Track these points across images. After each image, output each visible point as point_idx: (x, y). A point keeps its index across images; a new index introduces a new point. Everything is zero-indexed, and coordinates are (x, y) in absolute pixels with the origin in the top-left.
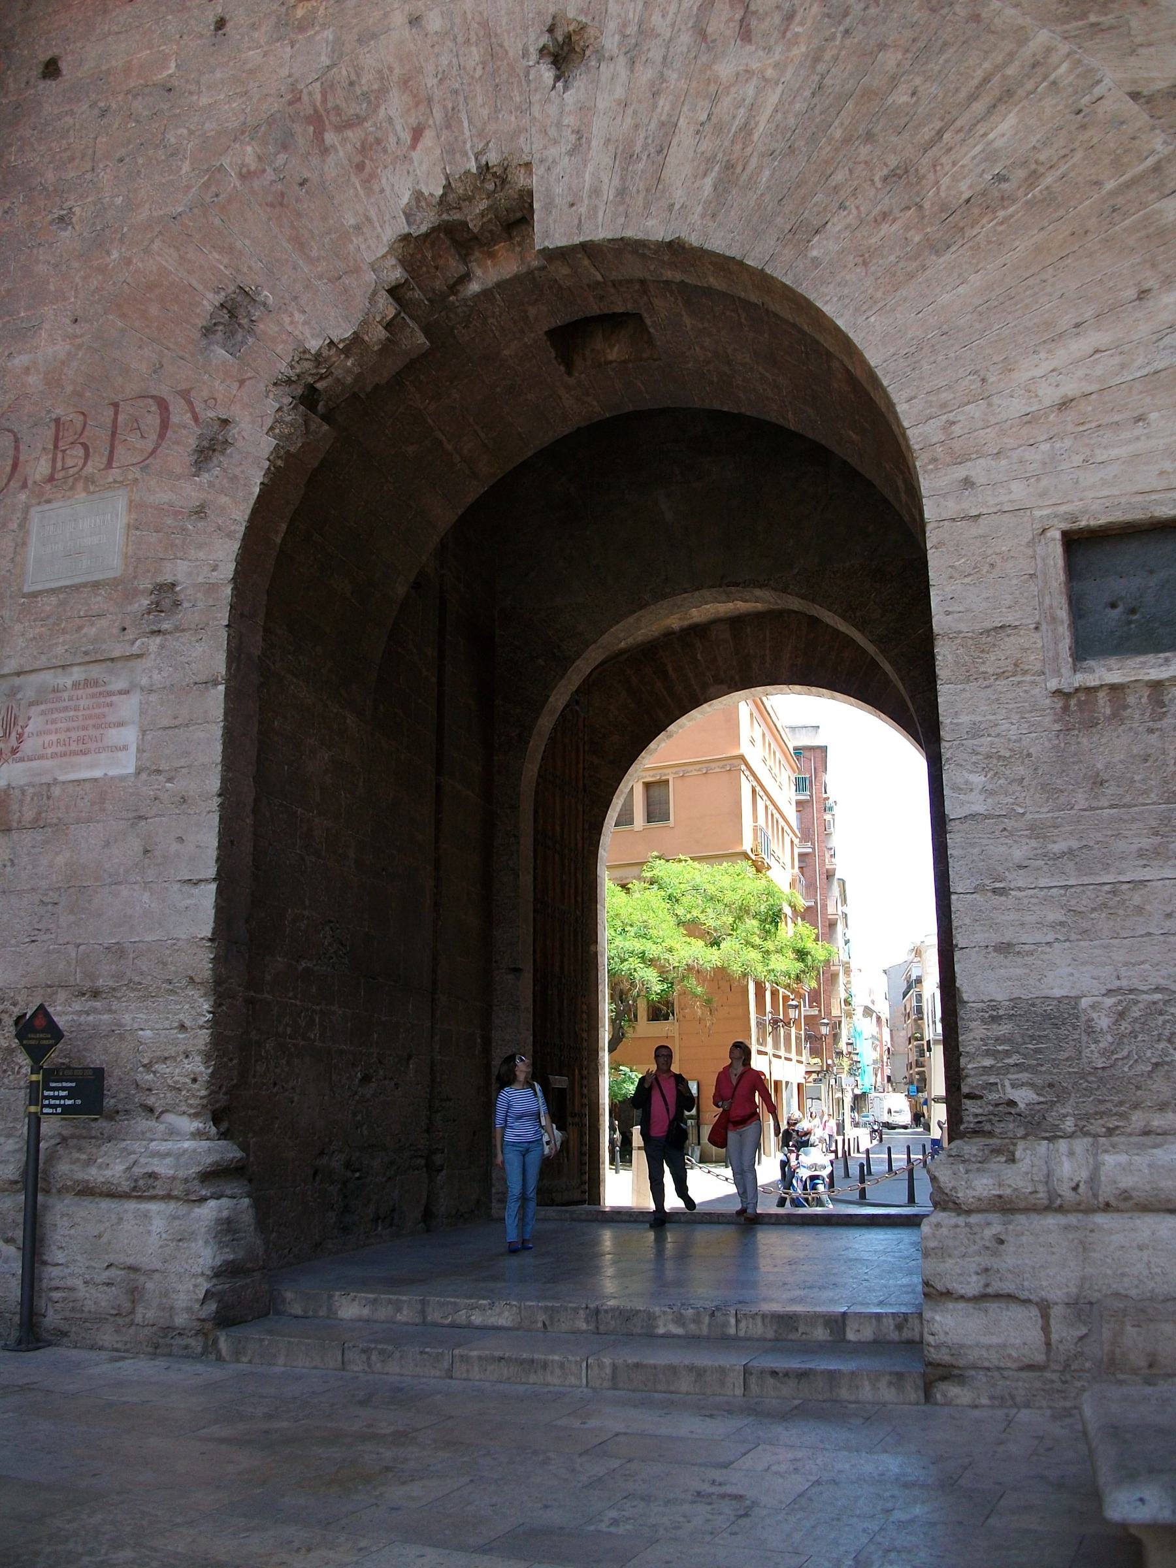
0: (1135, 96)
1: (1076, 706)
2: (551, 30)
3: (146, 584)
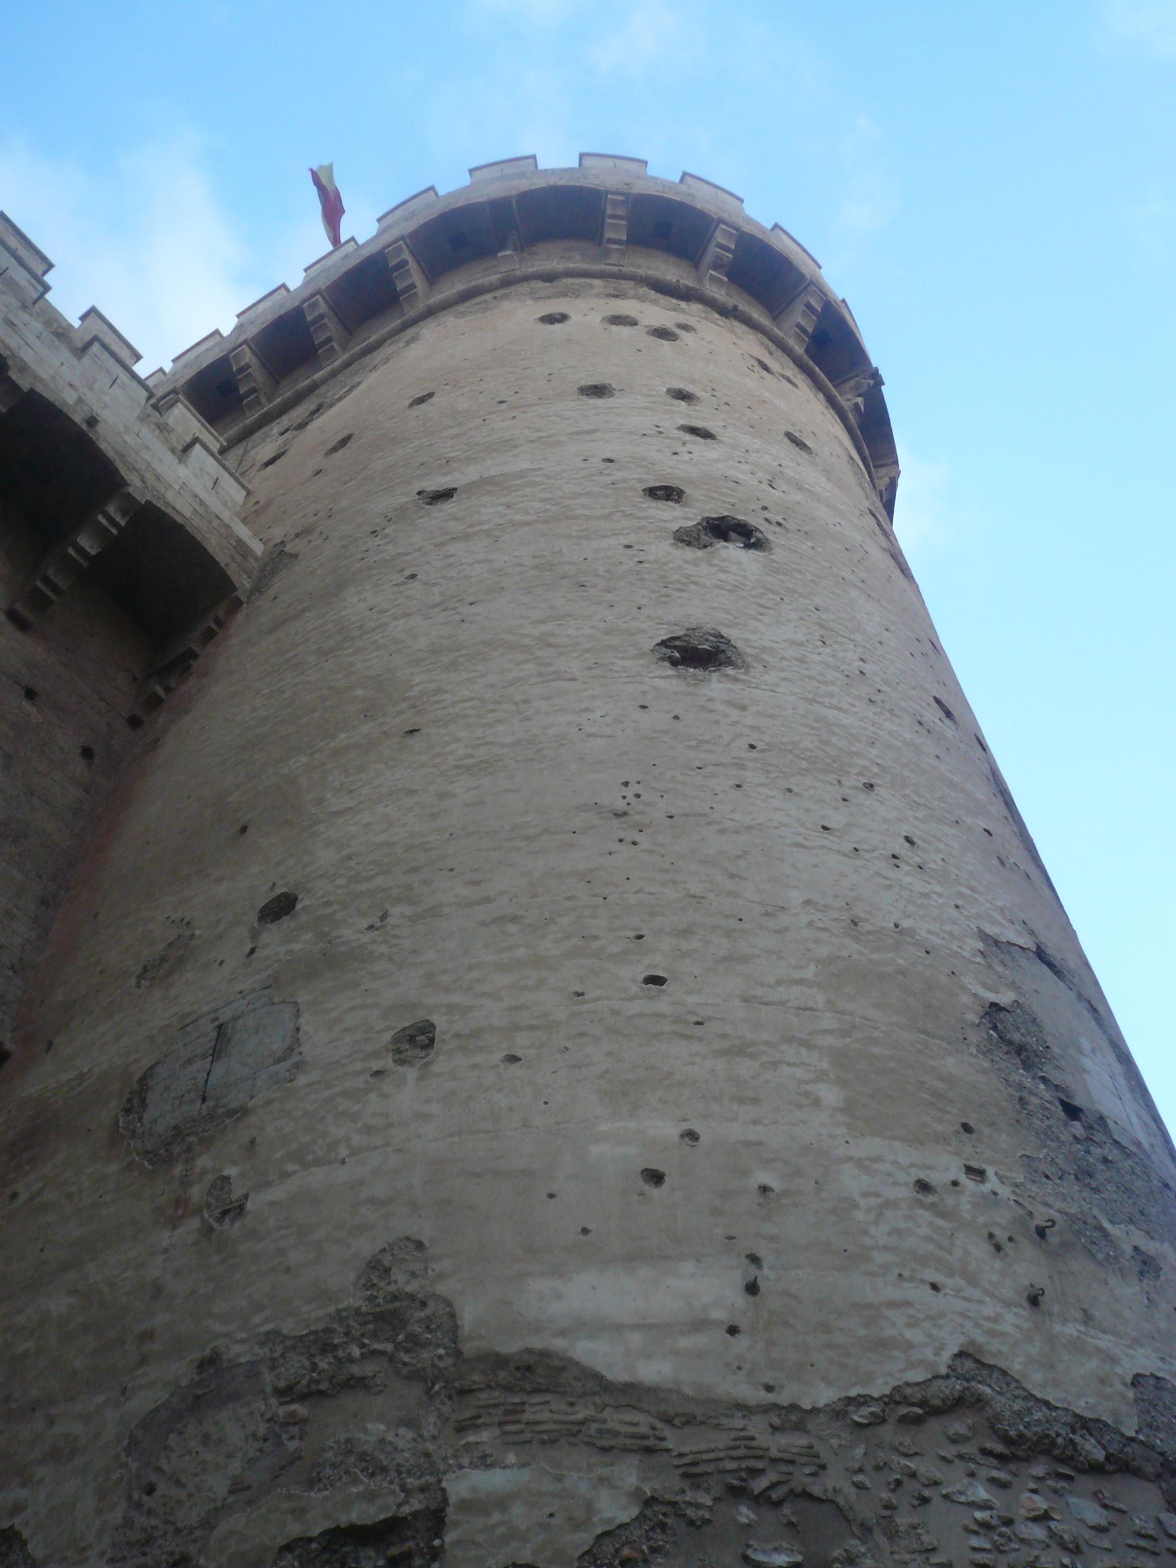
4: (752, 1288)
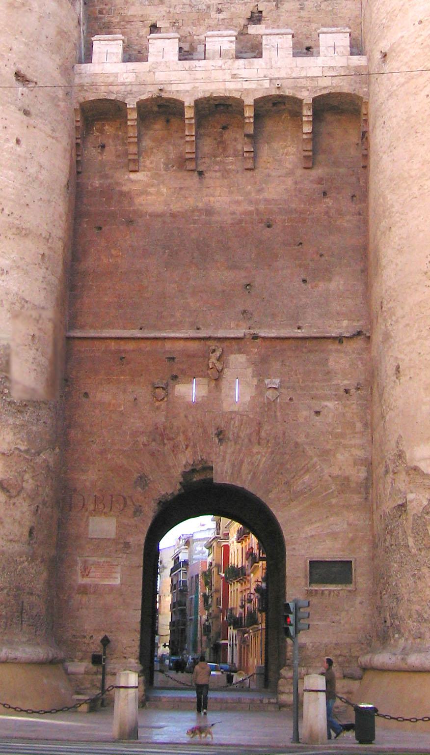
0: (330, 476)
2: (218, 429)
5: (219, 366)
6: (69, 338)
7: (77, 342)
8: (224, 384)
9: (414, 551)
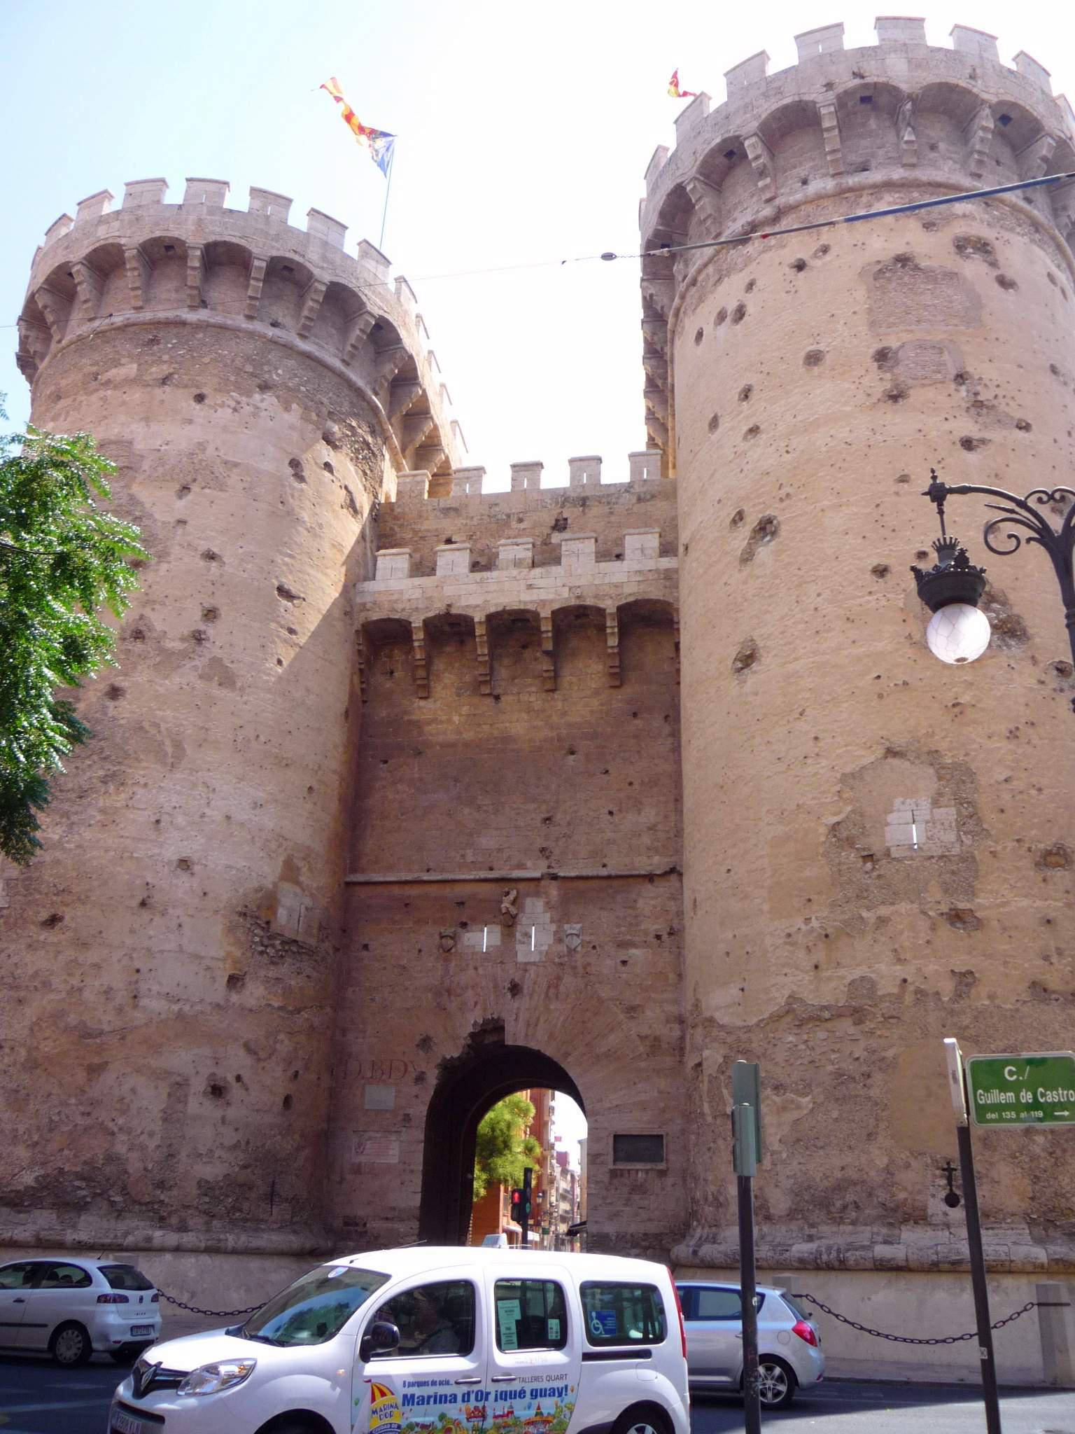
1: (614, 1174)
3: (401, 1112)
4: (743, 990)
5: (513, 911)
6: (348, 884)
7: (357, 888)
8: (519, 930)
9: (709, 1119)
